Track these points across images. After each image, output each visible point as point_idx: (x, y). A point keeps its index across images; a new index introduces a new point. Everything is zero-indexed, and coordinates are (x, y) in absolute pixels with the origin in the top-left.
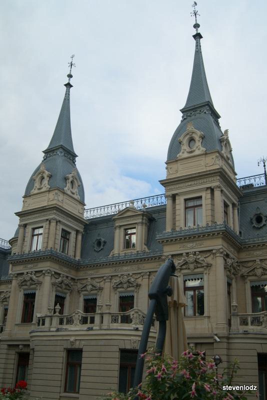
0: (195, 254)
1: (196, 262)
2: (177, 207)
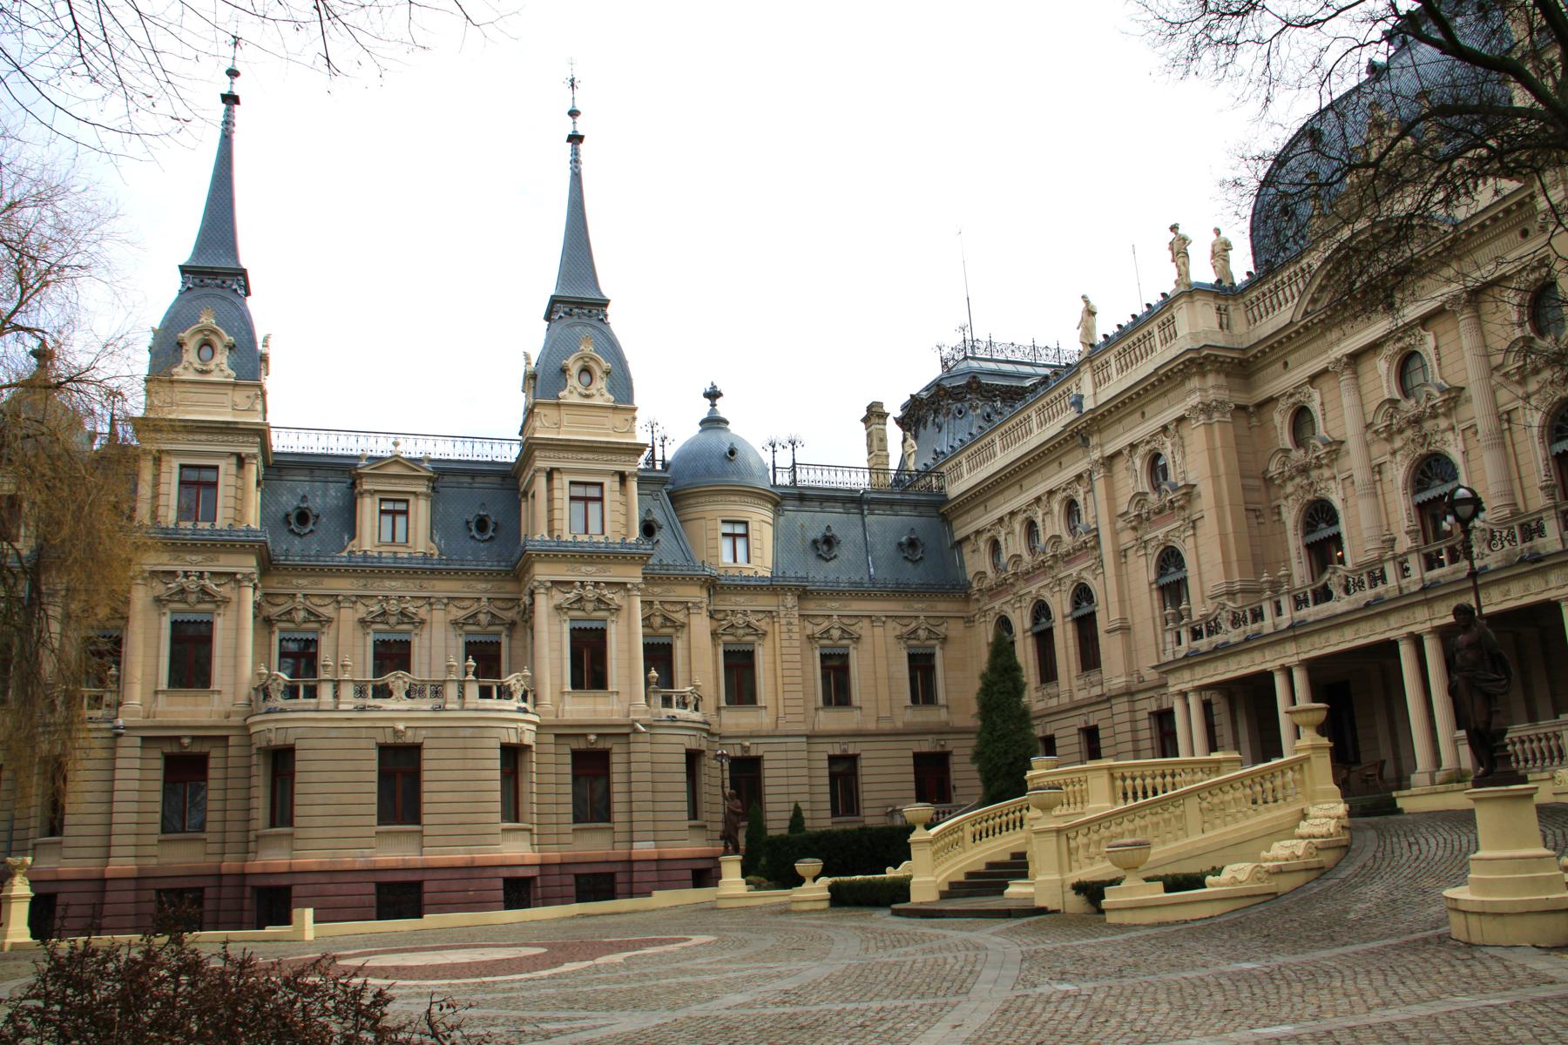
0: (596, 584)
1: (599, 600)
2: (557, 494)
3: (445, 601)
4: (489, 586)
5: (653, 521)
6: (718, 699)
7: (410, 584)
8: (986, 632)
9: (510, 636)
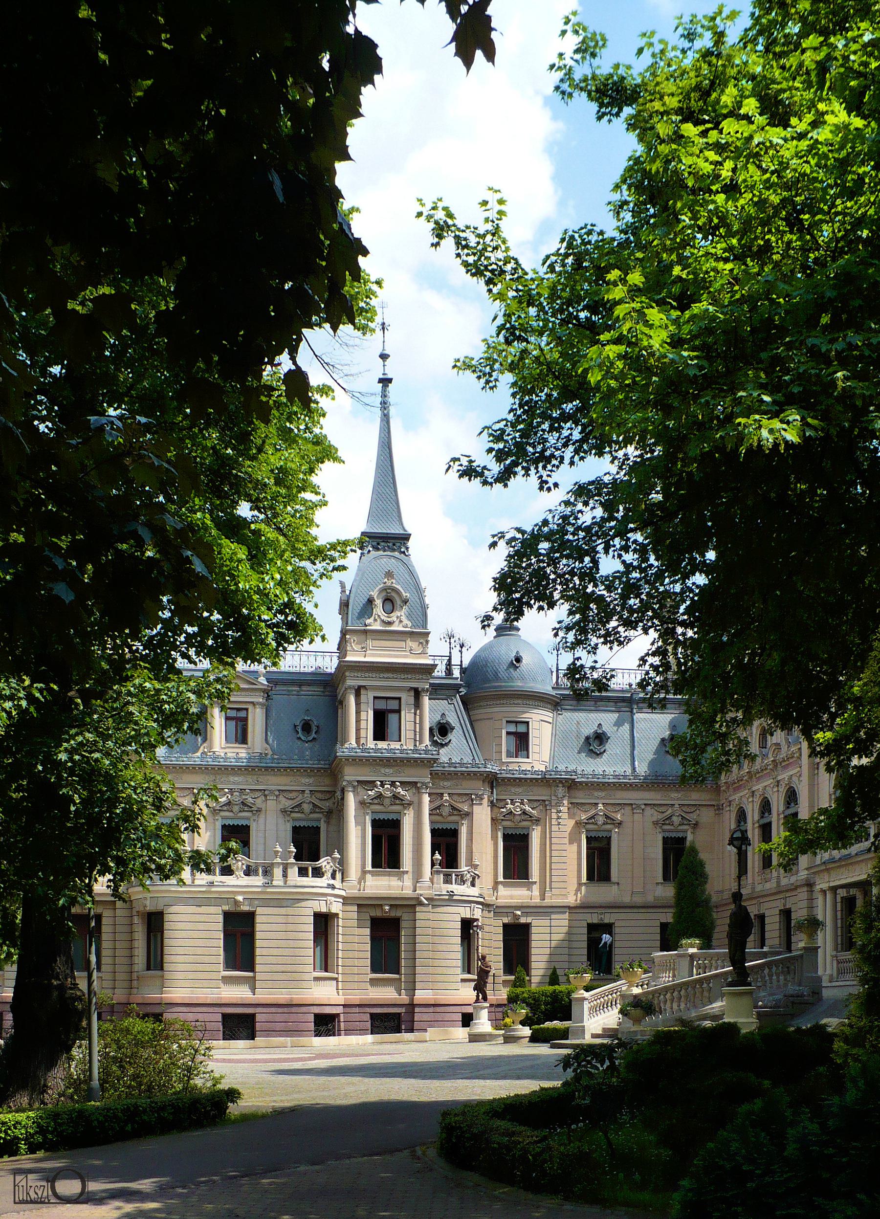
3: (277, 793)
4: (311, 780)
5: (448, 723)
6: (496, 875)
7: (250, 779)
8: (730, 821)
9: (328, 823)
